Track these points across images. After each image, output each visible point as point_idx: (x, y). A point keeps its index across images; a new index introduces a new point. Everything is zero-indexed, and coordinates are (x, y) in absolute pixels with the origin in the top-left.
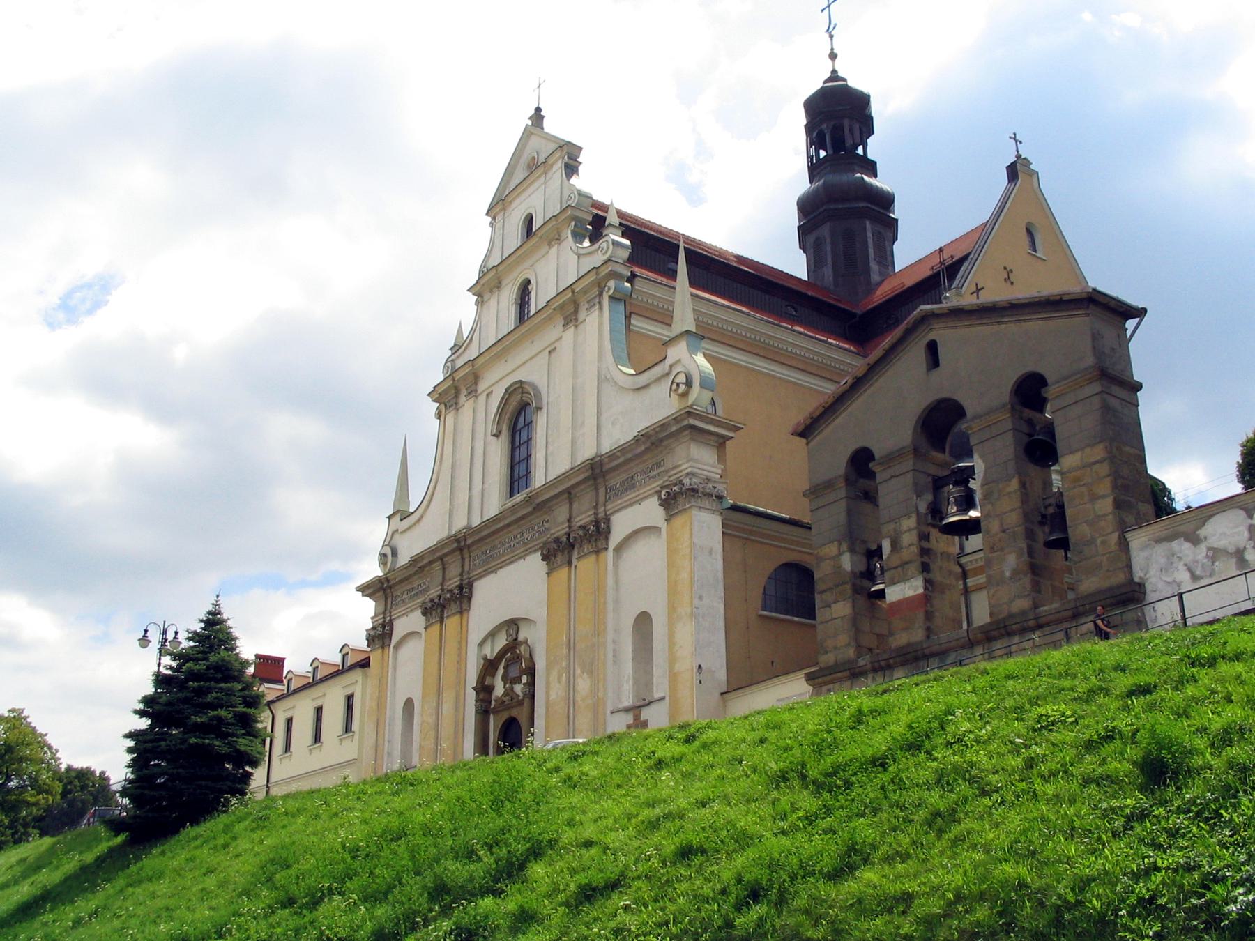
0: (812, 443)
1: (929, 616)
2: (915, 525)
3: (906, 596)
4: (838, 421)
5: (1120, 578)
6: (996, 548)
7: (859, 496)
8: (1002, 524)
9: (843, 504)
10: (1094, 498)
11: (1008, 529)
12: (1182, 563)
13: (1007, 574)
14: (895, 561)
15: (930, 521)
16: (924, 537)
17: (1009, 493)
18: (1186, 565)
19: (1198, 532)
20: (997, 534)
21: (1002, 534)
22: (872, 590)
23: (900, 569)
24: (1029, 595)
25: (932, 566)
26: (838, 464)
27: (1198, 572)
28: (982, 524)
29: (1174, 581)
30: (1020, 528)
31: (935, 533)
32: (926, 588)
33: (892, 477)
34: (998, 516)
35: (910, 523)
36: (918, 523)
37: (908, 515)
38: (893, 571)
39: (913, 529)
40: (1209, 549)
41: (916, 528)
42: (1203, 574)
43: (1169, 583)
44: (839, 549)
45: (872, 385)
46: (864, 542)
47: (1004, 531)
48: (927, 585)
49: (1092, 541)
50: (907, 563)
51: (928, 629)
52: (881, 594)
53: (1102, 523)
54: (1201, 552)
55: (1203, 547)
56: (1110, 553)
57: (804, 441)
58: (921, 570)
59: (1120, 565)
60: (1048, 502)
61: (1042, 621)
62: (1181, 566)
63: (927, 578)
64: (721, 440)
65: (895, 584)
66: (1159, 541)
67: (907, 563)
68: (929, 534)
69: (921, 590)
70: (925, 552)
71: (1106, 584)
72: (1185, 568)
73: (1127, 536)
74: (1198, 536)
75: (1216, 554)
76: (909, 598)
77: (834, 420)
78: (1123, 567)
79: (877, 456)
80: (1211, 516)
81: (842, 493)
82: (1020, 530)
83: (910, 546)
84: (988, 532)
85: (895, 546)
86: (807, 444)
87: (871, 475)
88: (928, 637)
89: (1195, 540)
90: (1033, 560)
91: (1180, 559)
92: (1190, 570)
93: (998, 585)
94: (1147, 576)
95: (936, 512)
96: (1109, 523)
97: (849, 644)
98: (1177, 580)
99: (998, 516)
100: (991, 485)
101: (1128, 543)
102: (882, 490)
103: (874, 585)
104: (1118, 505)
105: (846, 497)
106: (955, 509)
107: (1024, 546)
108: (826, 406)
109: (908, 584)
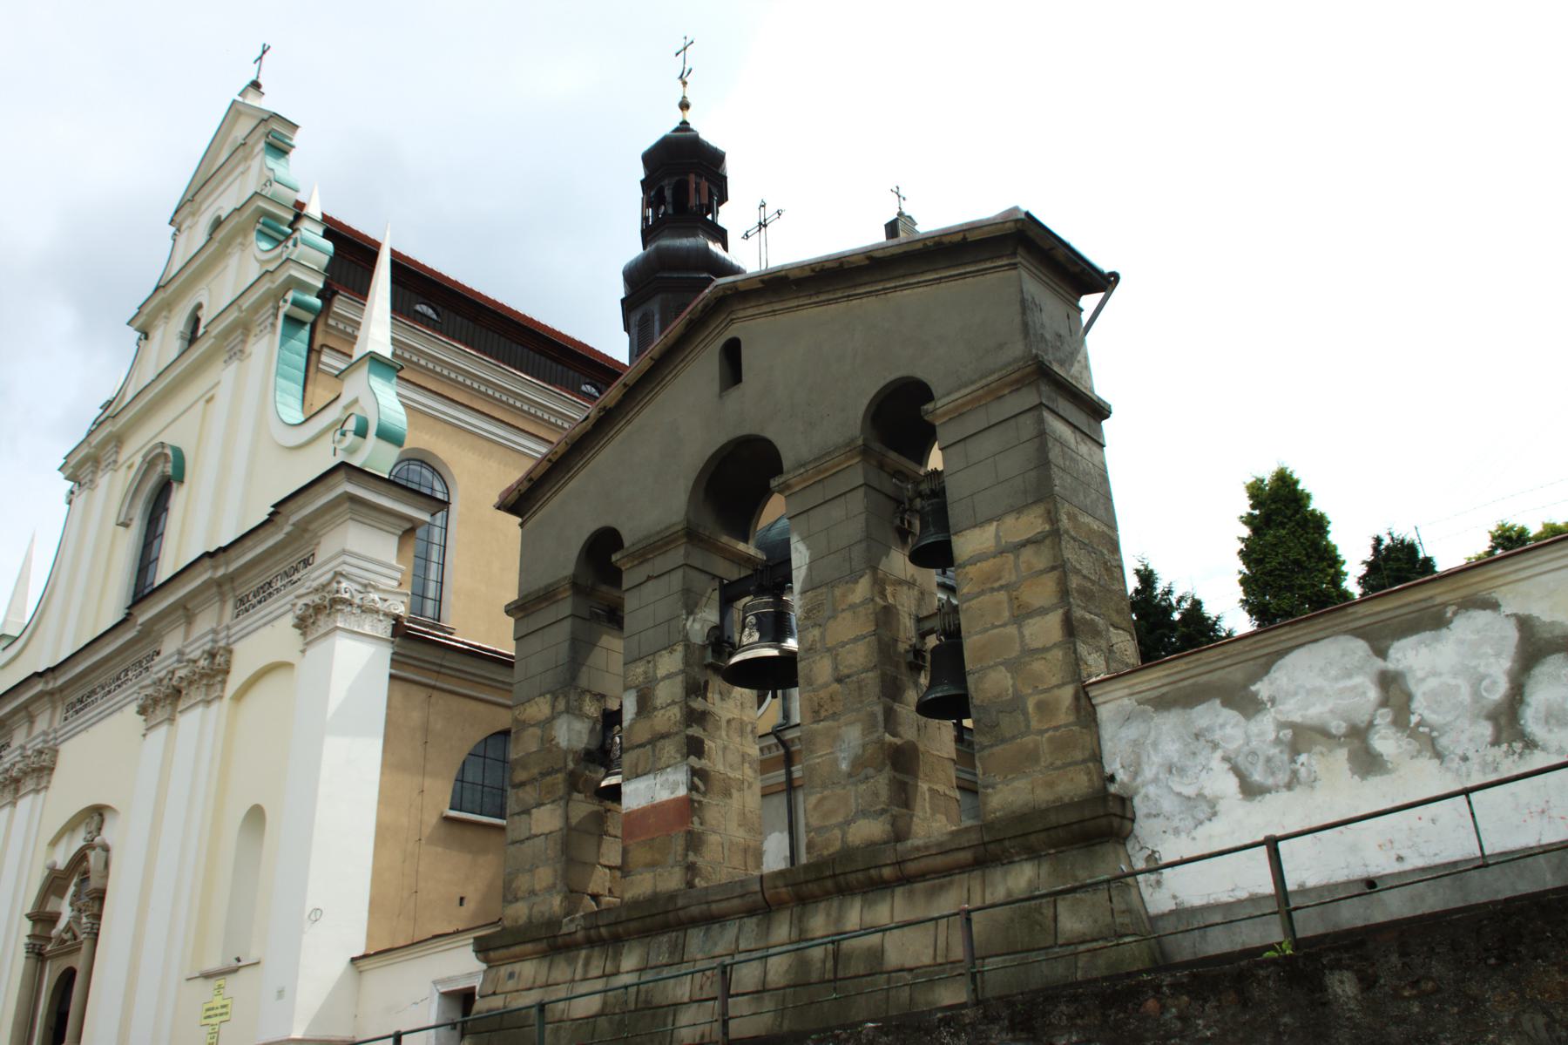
0: (529, 525)
1: (694, 842)
2: (681, 666)
4: (571, 484)
5: (1076, 784)
6: (823, 713)
7: (597, 614)
8: (836, 668)
9: (567, 626)
10: (1022, 614)
11: (848, 676)
12: (1219, 754)
13: (844, 766)
14: (642, 734)
15: (710, 660)
16: (696, 689)
17: (852, 607)
18: (1226, 759)
19: (1253, 688)
20: (826, 685)
21: (836, 686)
22: (603, 784)
23: (649, 747)
24: (883, 812)
25: (708, 744)
26: (565, 561)
27: (1257, 776)
28: (800, 666)
29: (1201, 796)
30: (871, 674)
31: (717, 683)
32: (692, 787)
33: (649, 578)
34: (829, 650)
35: (670, 663)
36: (687, 662)
37: (670, 648)
38: (641, 750)
39: (676, 674)
40: (1282, 725)
41: (682, 671)
42: (1270, 781)
43: (1189, 798)
44: (553, 707)
45: (629, 422)
46: (601, 697)
47: (839, 680)
48: (696, 780)
49: (1015, 705)
50: (664, 736)
51: (691, 869)
52: (615, 793)
53: (1038, 666)
56: (1056, 728)
57: (519, 520)
58: (685, 751)
59: (1079, 756)
60: (927, 625)
61: (912, 868)
63: (697, 766)
64: (408, 526)
65: (638, 776)
66: (1162, 703)
67: (664, 736)
68: (706, 683)
69: (682, 791)
70: (696, 717)
71: (1043, 796)
72: (1226, 766)
73: (1091, 695)
74: (1255, 695)
75: (1301, 738)
76: (662, 805)
77: (566, 483)
78: (1084, 761)
79: (627, 543)
80: (1282, 654)
81: (565, 607)
82: (871, 678)
83: (668, 705)
84: (810, 682)
85: (645, 705)
86: (522, 525)
87: (613, 576)
88: (690, 885)
89: (1248, 705)
91: (1215, 746)
92: (1236, 770)
93: (824, 786)
94: (1139, 780)
95: (721, 642)
96: (1050, 669)
97: (554, 886)
98: (1207, 792)
99: (829, 650)
100: (819, 591)
101: (1093, 707)
102: (630, 603)
103: (607, 775)
104: (1070, 628)
105: (572, 615)
106: (756, 636)
107: (878, 710)
108: (554, 459)
109: (660, 779)
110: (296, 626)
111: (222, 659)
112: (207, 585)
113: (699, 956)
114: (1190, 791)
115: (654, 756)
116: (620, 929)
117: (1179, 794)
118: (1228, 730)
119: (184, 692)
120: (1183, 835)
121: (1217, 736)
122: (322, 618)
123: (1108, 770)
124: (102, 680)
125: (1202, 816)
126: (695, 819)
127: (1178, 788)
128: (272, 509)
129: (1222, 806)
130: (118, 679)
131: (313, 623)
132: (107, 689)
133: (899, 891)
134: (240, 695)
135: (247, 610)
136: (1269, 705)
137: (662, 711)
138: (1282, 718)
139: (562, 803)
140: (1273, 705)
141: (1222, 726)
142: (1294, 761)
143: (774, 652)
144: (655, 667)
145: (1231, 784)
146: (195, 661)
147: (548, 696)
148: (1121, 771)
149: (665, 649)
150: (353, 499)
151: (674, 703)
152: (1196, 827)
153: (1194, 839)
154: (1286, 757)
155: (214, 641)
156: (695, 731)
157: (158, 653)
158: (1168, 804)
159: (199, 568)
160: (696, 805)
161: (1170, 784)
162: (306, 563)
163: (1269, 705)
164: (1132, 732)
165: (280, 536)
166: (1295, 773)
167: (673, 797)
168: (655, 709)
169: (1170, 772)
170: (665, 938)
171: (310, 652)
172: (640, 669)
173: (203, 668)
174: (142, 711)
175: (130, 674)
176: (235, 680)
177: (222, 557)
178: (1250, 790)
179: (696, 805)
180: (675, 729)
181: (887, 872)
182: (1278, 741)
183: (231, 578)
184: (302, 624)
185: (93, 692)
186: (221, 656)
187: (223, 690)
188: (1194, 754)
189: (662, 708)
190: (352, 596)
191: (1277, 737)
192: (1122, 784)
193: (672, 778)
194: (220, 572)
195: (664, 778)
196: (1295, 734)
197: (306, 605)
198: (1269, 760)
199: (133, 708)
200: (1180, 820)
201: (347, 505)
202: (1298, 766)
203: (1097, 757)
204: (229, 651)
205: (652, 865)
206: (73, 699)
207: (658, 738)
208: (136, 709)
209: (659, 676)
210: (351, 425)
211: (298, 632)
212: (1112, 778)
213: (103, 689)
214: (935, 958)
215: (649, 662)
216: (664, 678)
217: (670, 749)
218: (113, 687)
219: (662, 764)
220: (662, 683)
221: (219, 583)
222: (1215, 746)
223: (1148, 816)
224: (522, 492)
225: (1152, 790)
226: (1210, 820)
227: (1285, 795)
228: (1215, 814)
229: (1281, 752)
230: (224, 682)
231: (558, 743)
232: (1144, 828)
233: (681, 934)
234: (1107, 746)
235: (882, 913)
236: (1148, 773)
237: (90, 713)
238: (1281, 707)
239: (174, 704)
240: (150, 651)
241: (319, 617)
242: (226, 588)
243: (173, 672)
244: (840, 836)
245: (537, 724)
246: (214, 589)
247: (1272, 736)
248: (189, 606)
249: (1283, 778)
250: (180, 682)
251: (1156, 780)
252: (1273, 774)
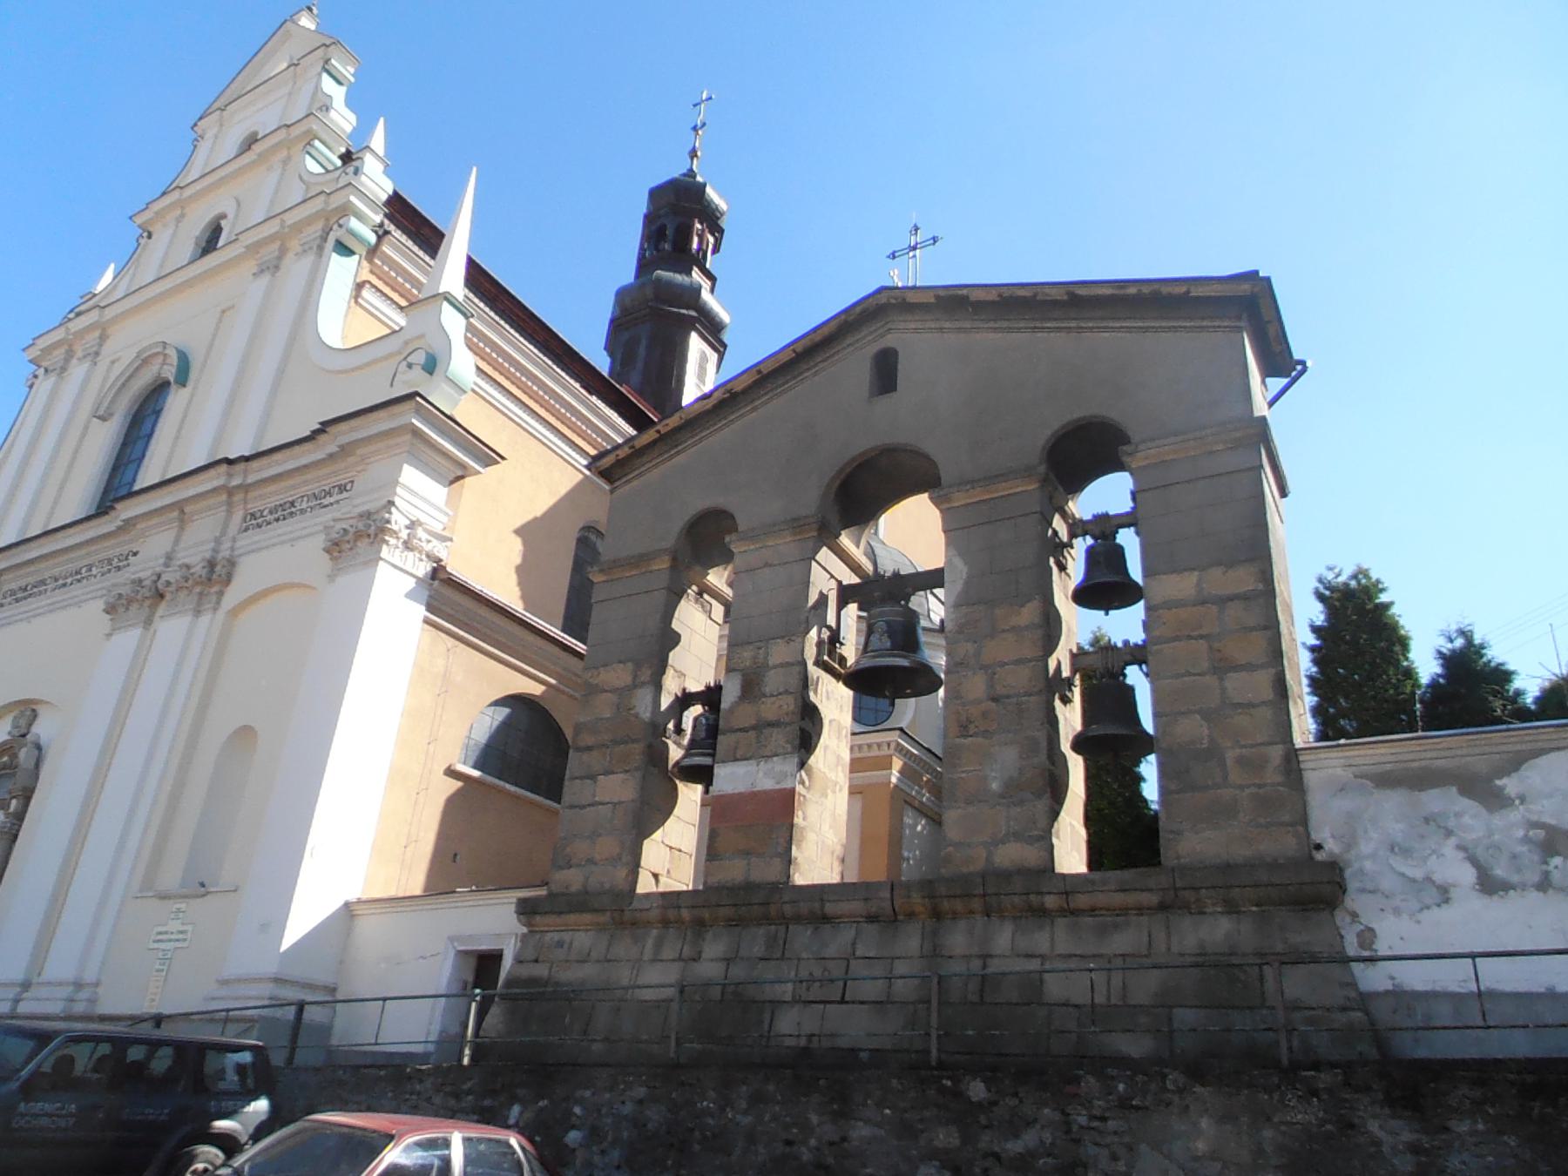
3: (759, 788)
12: (1453, 841)
18: (1461, 847)
23: (752, 734)
27: (1499, 872)
29: (1428, 879)
42: (1515, 878)
43: (1414, 881)
44: (635, 677)
50: (771, 724)
54: (1508, 827)
55: (1515, 815)
58: (797, 742)
62: (1449, 848)
65: (736, 760)
67: (771, 724)
72: (1461, 855)
83: (780, 694)
90: (1052, 768)
92: (1474, 861)
98: (1435, 877)
110: (327, 551)
111: (224, 571)
112: (215, 490)
113: (804, 955)
114: (1418, 874)
115: (759, 742)
116: (706, 914)
117: (1403, 875)
118: (1467, 820)
119: (168, 597)
120: (1405, 916)
121: (1451, 823)
122: (363, 544)
123: (1316, 837)
124: (56, 571)
125: (1428, 901)
126: (800, 813)
127: (1403, 869)
128: (318, 426)
129: (1454, 893)
130: (78, 573)
131: (351, 549)
132: (61, 582)
133: (1061, 922)
134: (235, 612)
135: (259, 526)
136: (1517, 802)
137: (774, 699)
138: (1534, 818)
139: (638, 774)
140: (1522, 802)
141: (1458, 815)
142: (1546, 863)
143: (905, 663)
144: (767, 654)
145: (1468, 875)
146: (188, 567)
147: (630, 665)
148: (1331, 840)
149: (783, 637)
150: (416, 433)
151: (787, 692)
152: (1422, 909)
153: (1418, 922)
154: (1536, 858)
155: (215, 551)
156: (807, 725)
157: (135, 554)
158: (1387, 883)
159: (212, 472)
160: (802, 798)
161: (1391, 861)
162: (342, 488)
163: (1517, 802)
164: (1344, 804)
165: (320, 455)
166: (1546, 874)
167: (778, 787)
168: (765, 696)
169: (1392, 849)
170: (761, 931)
171: (343, 580)
172: (747, 654)
173: (200, 576)
174: (110, 610)
175: (94, 571)
176: (233, 595)
177: (241, 466)
178: (1489, 885)
179: (802, 798)
180: (787, 719)
181: (1051, 901)
182: (1526, 840)
183: (245, 488)
184: (336, 548)
185: (43, 582)
186: (224, 566)
187: (218, 602)
188: (1423, 837)
189: (772, 696)
190: (400, 530)
191: (1526, 836)
192: (1331, 853)
193: (778, 768)
194: (236, 482)
195: (769, 765)
196: (1547, 833)
197: (345, 530)
198: (1514, 857)
199: (100, 604)
200: (1403, 900)
201: (408, 437)
202: (1551, 868)
203: (1304, 820)
204: (232, 563)
205: (747, 853)
206: (14, 586)
207: (761, 726)
208: (103, 607)
209: (770, 663)
210: (419, 358)
211: (327, 556)
212: (1319, 847)
213: (56, 580)
214: (1109, 998)
215: (760, 648)
216: (775, 667)
217: (778, 738)
218: (69, 581)
219: (767, 753)
220: (773, 672)
221: (231, 492)
222: (1449, 833)
223: (1363, 890)
224: (620, 458)
225: (1368, 865)
226: (1439, 905)
227: (1534, 896)
228: (1447, 901)
229: (1530, 851)
230: (221, 594)
231: (638, 714)
232: (1353, 900)
233: (782, 929)
234: (1316, 814)
235: (1041, 940)
236: (1365, 848)
237: (32, 604)
238: (1531, 806)
239: (153, 607)
240: (125, 549)
241: (359, 544)
242: (238, 497)
243: (159, 576)
244: (985, 855)
245: (614, 691)
246: (224, 497)
247: (1520, 833)
248: (187, 509)
249: (1534, 877)
250: (167, 586)
251: (1373, 856)
252: (1519, 870)
